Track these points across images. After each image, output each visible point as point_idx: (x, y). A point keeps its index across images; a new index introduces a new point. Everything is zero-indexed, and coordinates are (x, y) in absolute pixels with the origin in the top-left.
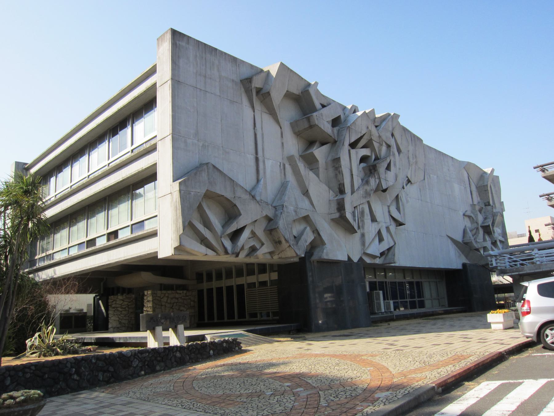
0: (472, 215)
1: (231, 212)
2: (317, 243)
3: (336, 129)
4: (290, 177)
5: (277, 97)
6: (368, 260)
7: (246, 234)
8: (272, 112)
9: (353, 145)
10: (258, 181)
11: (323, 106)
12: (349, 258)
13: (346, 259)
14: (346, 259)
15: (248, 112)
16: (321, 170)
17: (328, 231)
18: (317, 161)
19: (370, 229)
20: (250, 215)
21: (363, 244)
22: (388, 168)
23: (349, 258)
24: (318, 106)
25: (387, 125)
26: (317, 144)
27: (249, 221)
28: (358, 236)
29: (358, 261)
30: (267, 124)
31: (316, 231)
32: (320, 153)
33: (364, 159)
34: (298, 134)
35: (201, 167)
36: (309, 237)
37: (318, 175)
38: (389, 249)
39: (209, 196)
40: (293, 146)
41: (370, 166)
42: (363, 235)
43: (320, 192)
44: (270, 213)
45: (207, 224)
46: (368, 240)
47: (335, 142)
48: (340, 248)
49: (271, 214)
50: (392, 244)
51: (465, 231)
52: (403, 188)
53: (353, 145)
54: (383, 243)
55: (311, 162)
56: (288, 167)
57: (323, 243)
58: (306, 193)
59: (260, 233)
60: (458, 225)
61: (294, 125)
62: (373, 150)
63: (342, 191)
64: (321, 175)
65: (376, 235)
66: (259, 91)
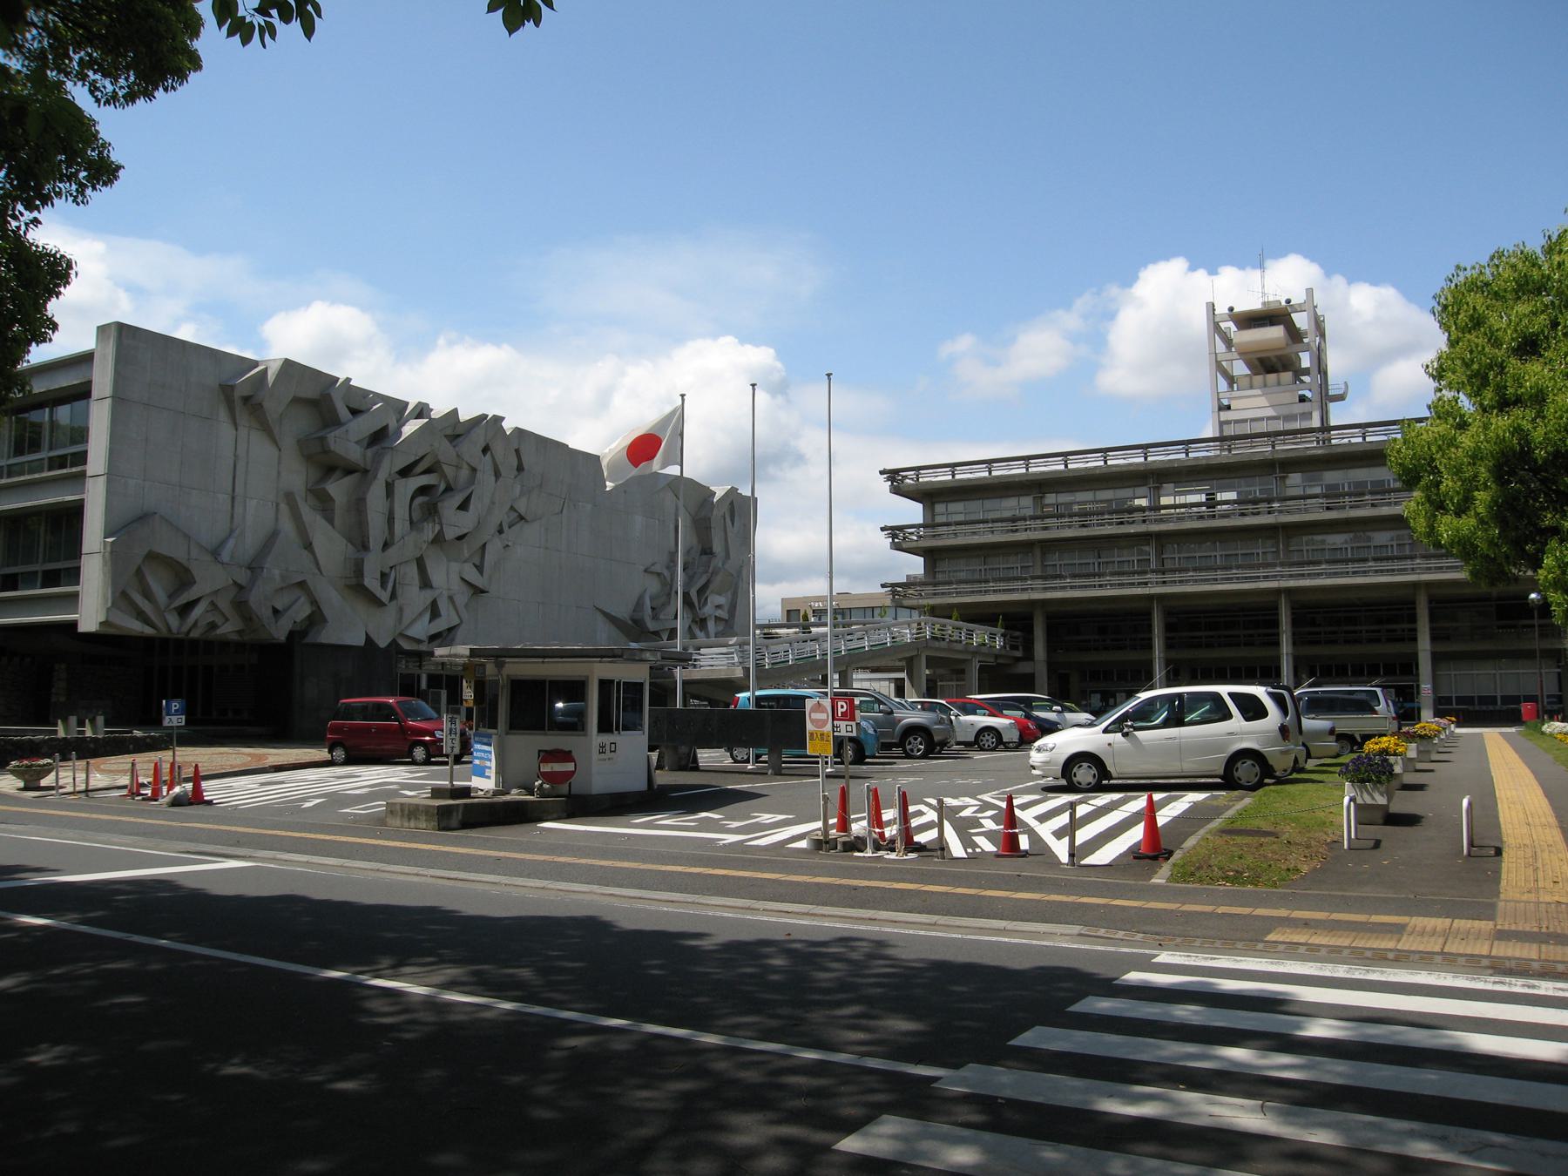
0: (666, 573)
1: (182, 577)
2: (317, 618)
3: (369, 453)
4: (287, 526)
5: (273, 408)
6: (406, 645)
7: (197, 612)
8: (266, 428)
9: (405, 472)
10: (232, 531)
11: (355, 412)
12: (369, 639)
13: (361, 641)
14: (361, 641)
15: (225, 429)
16: (338, 512)
17: (333, 599)
18: (332, 500)
19: (415, 598)
20: (209, 580)
21: (400, 620)
22: (464, 506)
23: (369, 639)
24: (344, 413)
25: (479, 438)
26: (338, 473)
27: (208, 591)
28: (392, 608)
29: (390, 645)
30: (259, 448)
31: (314, 602)
32: (338, 489)
33: (423, 490)
34: (308, 458)
35: (143, 518)
36: (303, 611)
37: (330, 521)
38: (450, 630)
39: (152, 557)
40: (297, 477)
41: (428, 502)
42: (401, 610)
43: (330, 545)
44: (242, 577)
45: (147, 594)
46: (408, 615)
47: (366, 471)
48: (349, 626)
49: (242, 580)
50: (456, 621)
51: (639, 604)
52: (501, 531)
53: (405, 472)
54: (437, 621)
55: (324, 503)
56: (283, 506)
57: (324, 620)
58: (308, 546)
59: (224, 604)
60: (628, 589)
61: (302, 443)
62: (443, 476)
63: (365, 547)
64: (337, 521)
65: (425, 610)
66: (246, 400)
